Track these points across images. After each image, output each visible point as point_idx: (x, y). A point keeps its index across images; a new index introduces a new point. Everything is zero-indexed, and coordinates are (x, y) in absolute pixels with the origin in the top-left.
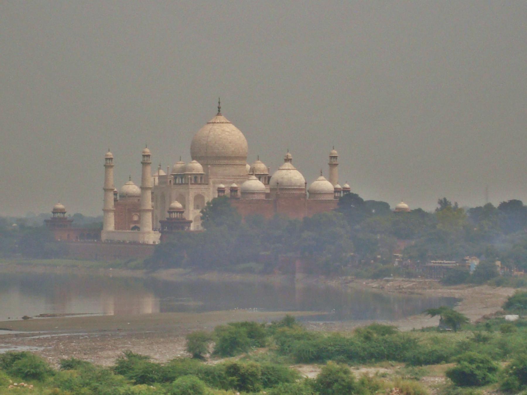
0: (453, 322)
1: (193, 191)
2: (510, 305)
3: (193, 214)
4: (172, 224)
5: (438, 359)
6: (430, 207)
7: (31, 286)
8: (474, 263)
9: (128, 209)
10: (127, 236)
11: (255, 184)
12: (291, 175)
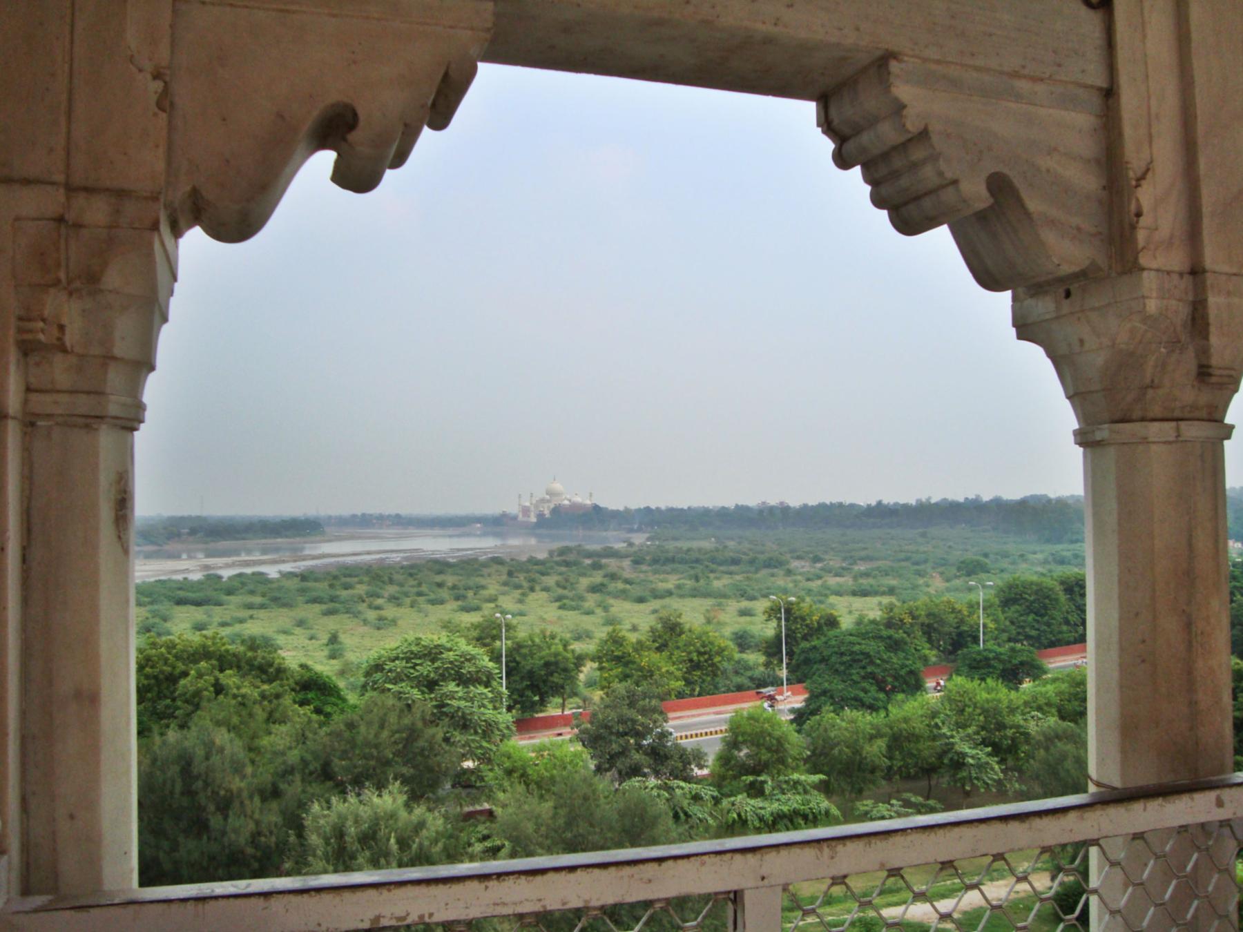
0: (631, 545)
1: (546, 505)
2: (648, 539)
3: (547, 512)
4: (540, 516)
5: (627, 556)
6: (621, 508)
7: (496, 535)
8: (636, 527)
9: (526, 511)
10: (525, 519)
11: (566, 502)
12: (578, 499)
